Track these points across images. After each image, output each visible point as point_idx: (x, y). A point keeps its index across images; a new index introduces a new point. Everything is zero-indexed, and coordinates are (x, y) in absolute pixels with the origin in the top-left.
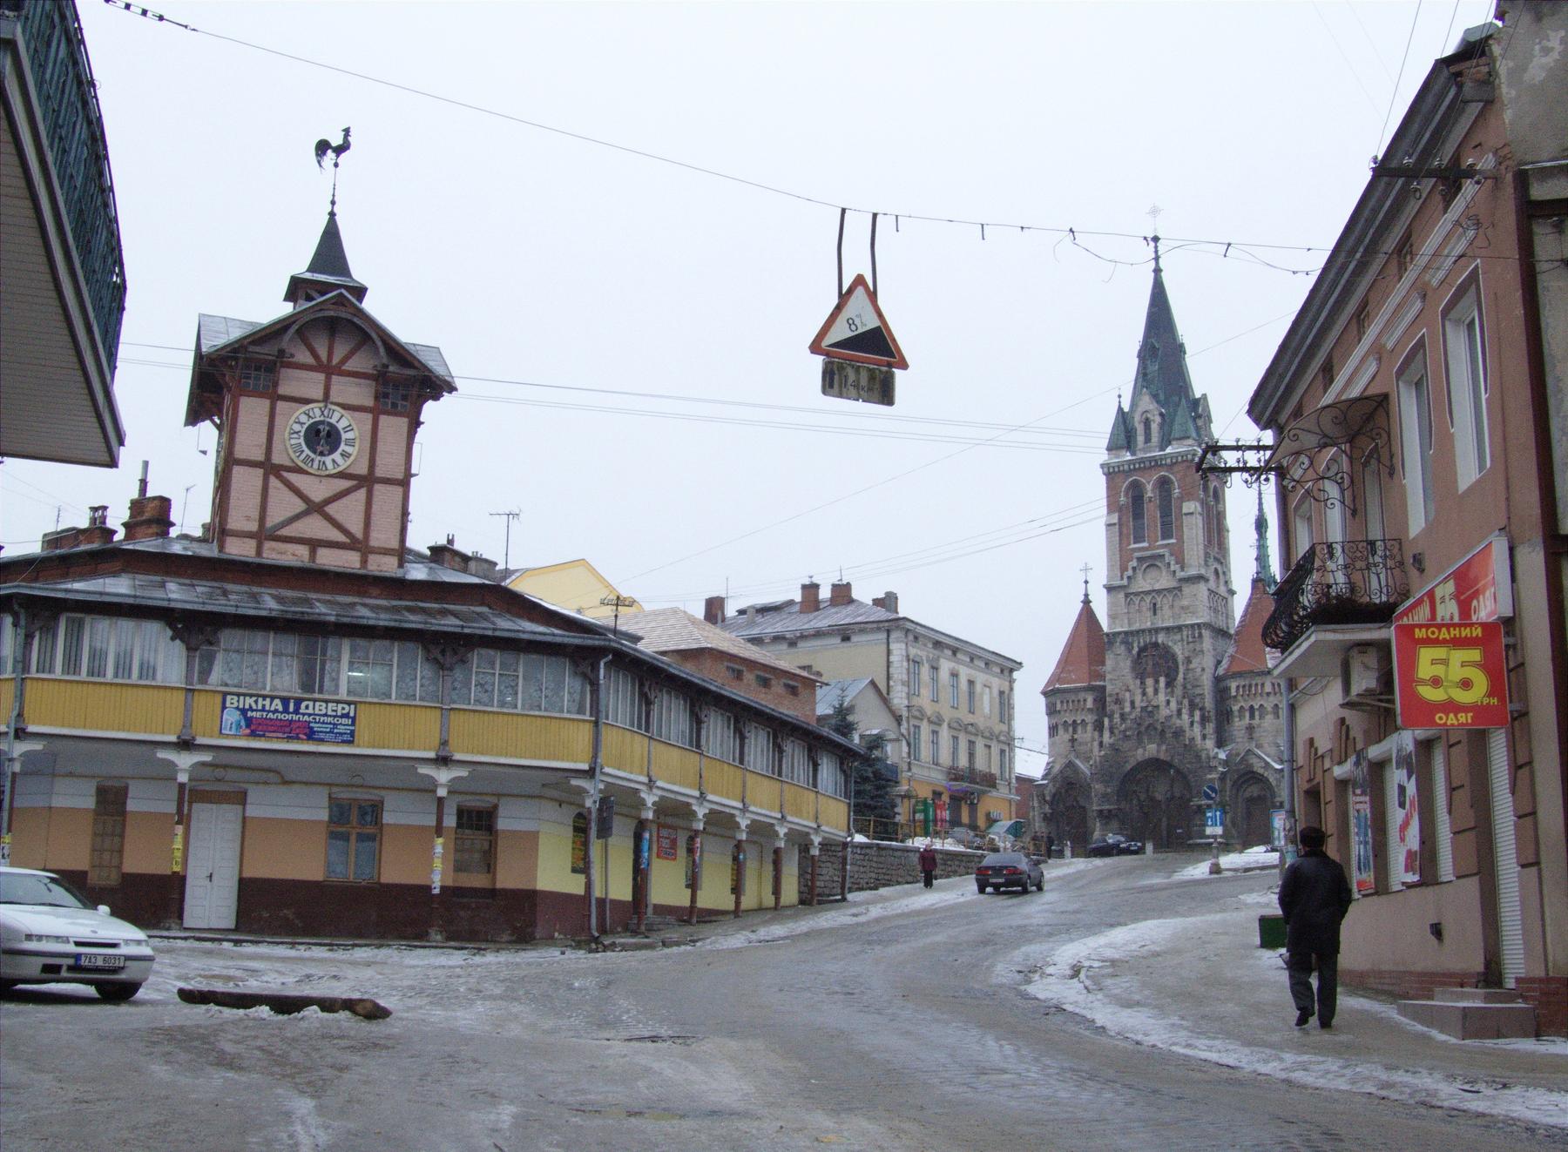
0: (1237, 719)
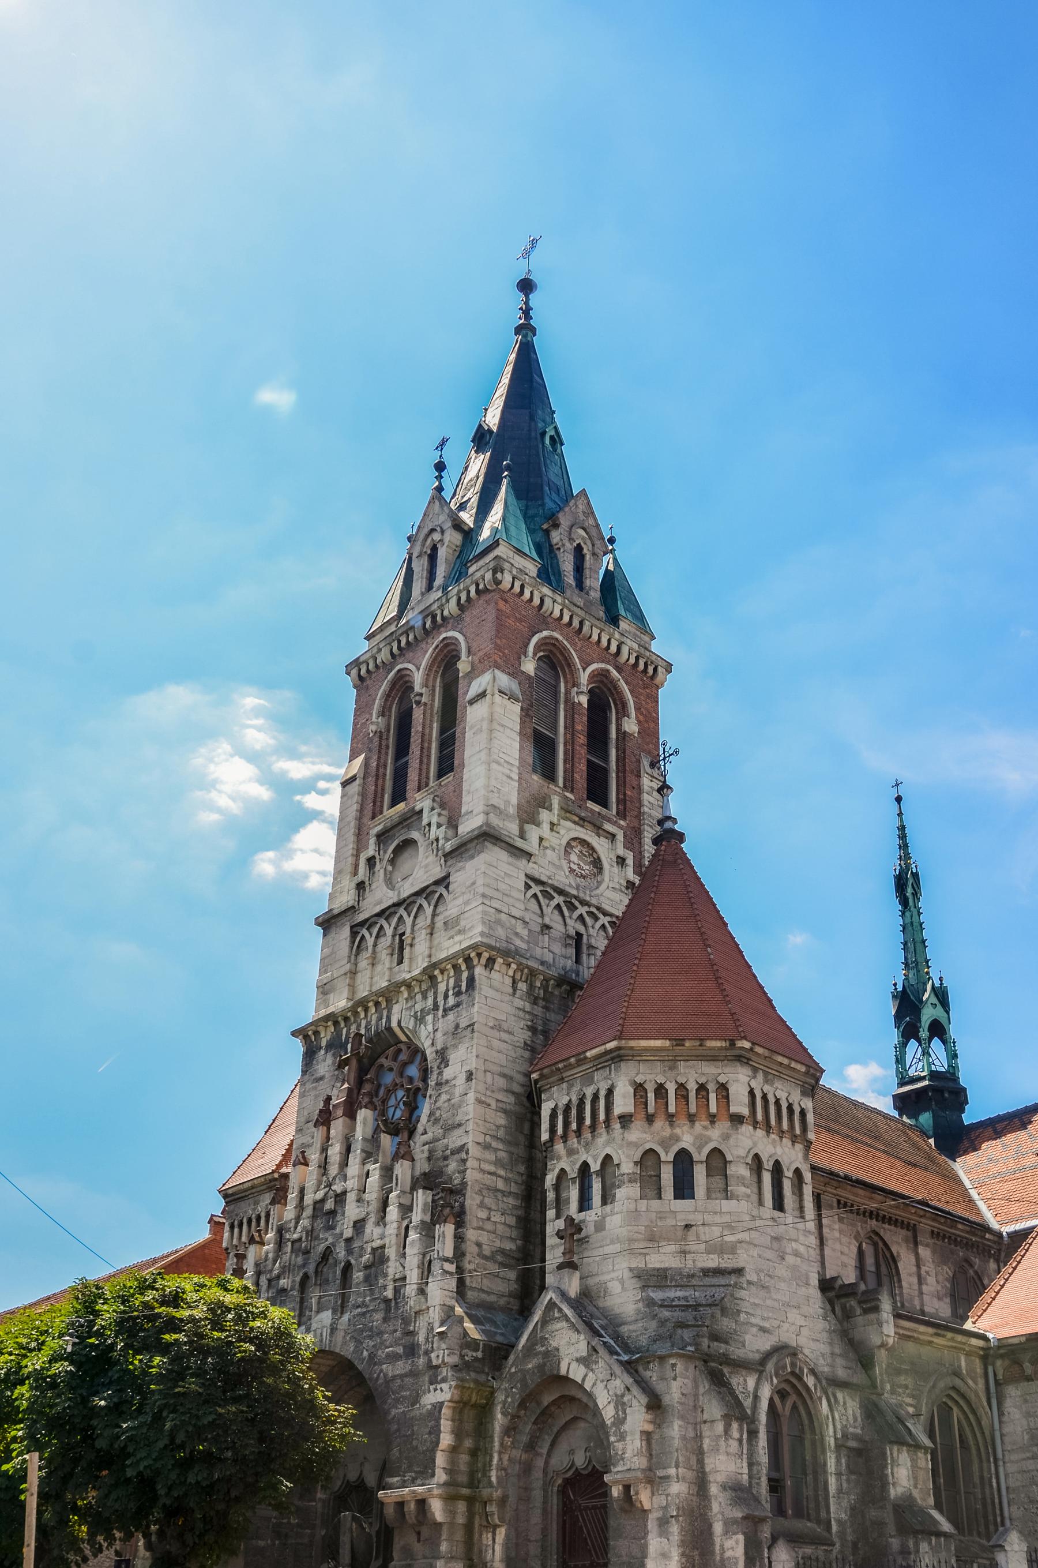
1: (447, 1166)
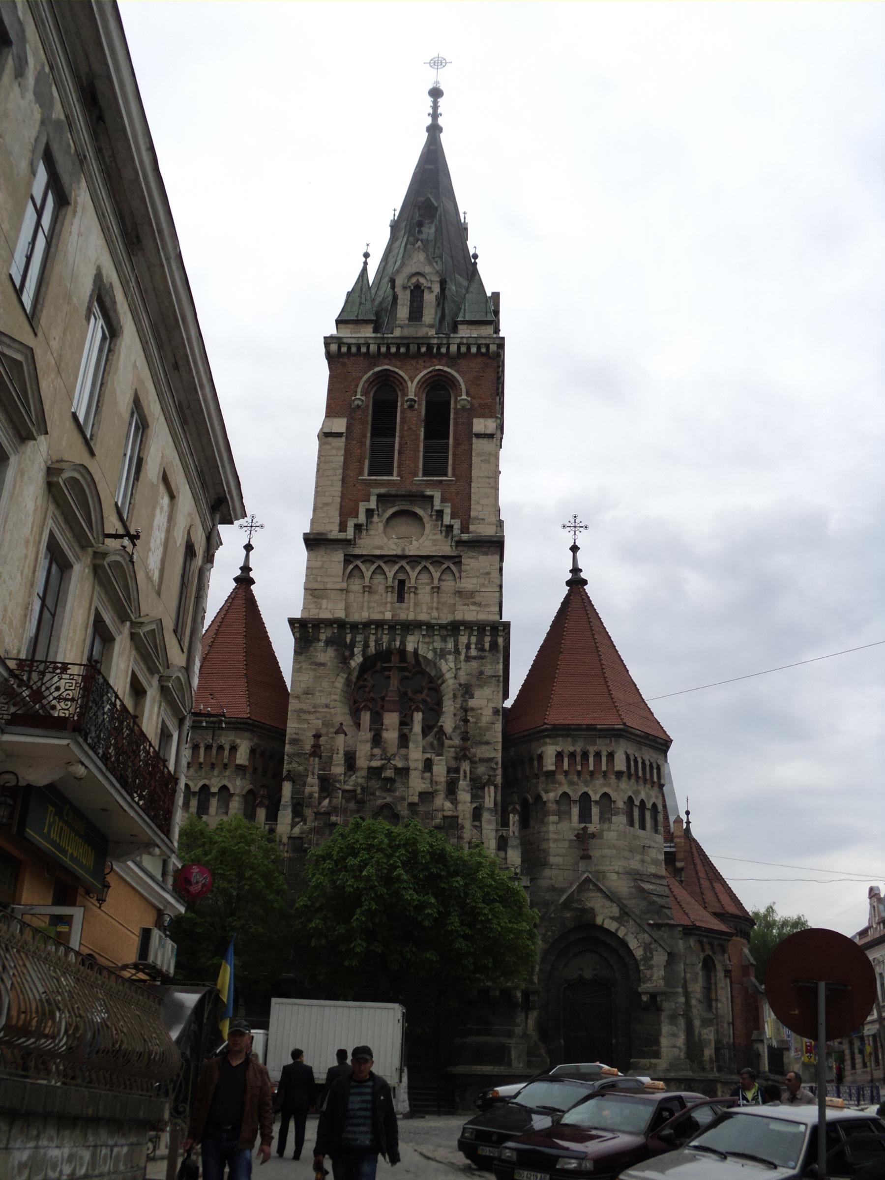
0: (553, 818)
1: (476, 768)
